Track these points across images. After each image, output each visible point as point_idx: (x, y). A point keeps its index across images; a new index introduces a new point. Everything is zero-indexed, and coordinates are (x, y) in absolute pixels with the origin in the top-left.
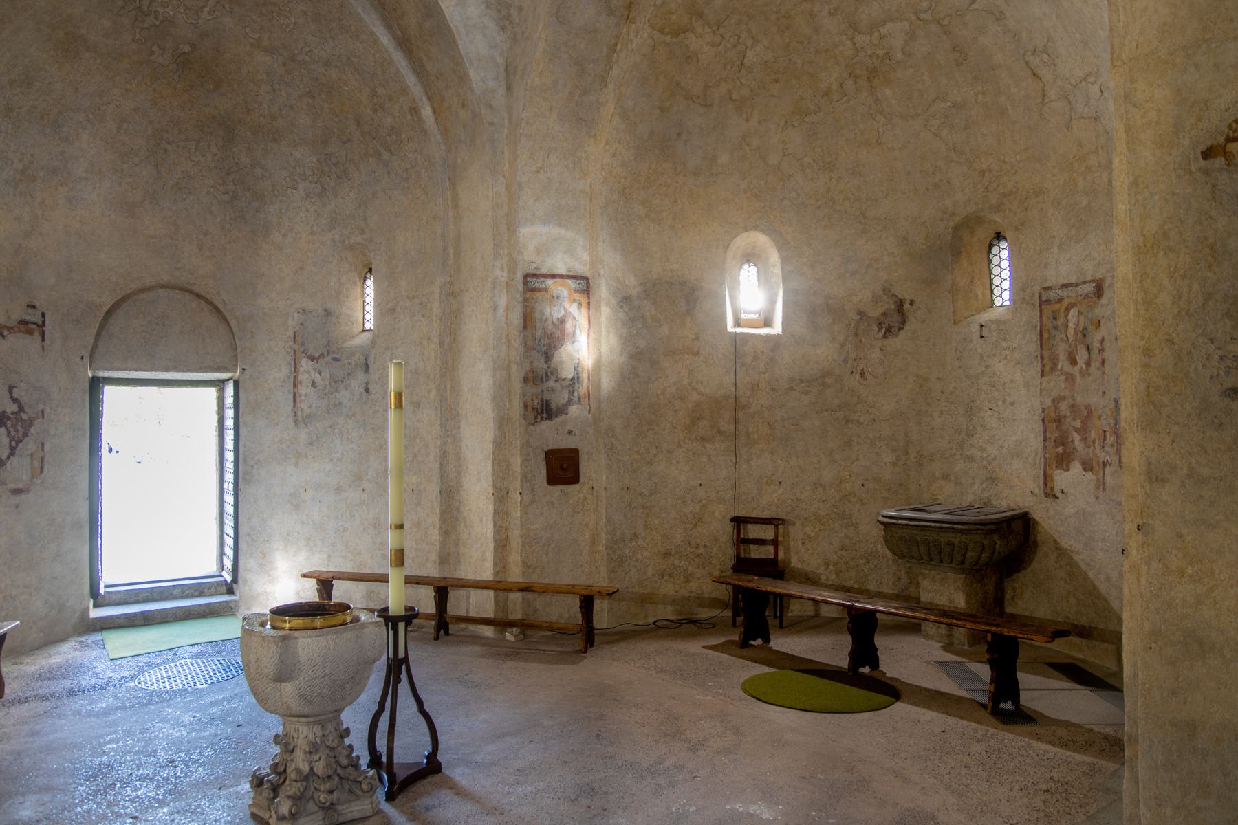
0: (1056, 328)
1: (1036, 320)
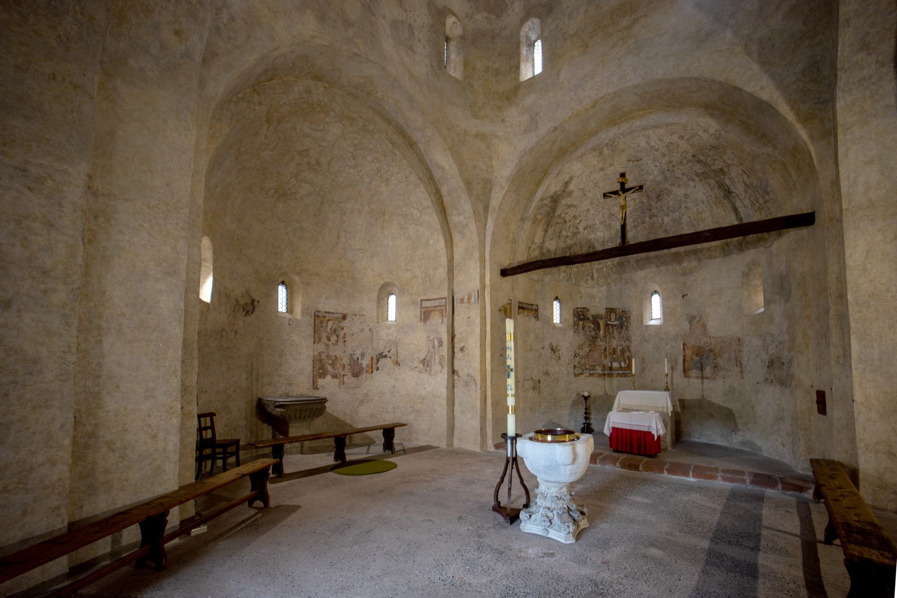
1: (312, 322)
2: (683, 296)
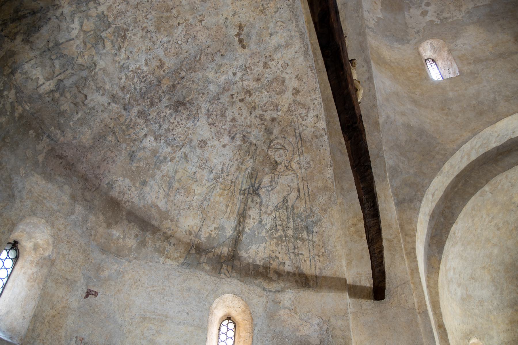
2: (89, 293)
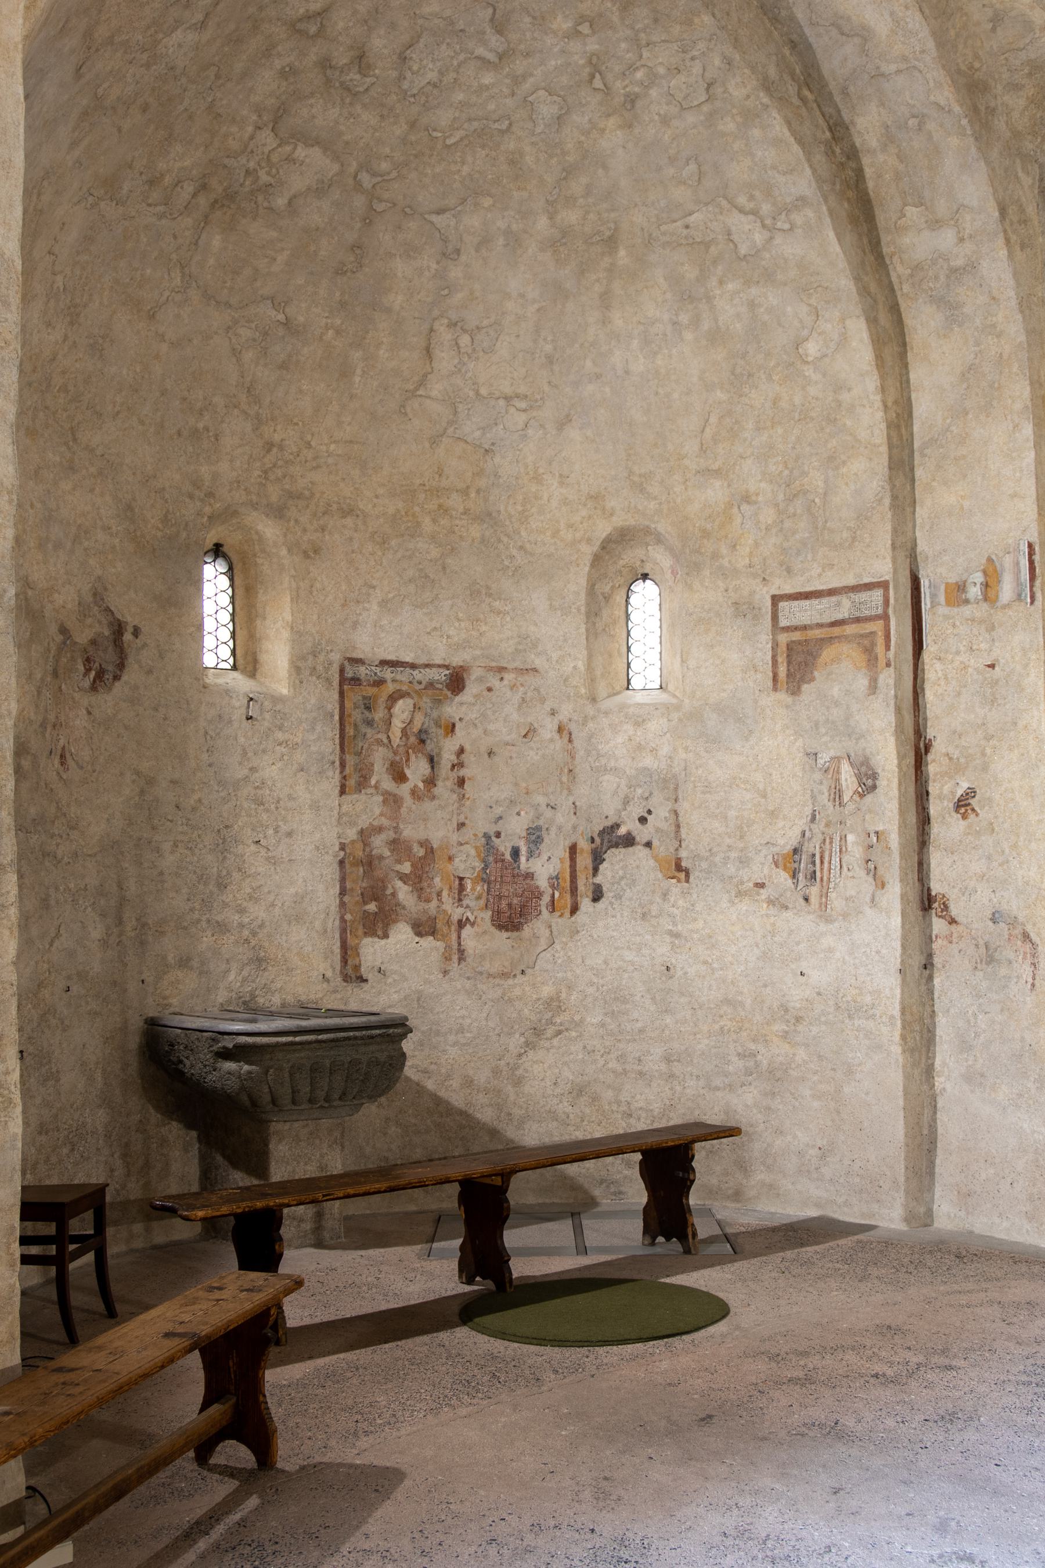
0: (370, 723)
1: (333, 706)
